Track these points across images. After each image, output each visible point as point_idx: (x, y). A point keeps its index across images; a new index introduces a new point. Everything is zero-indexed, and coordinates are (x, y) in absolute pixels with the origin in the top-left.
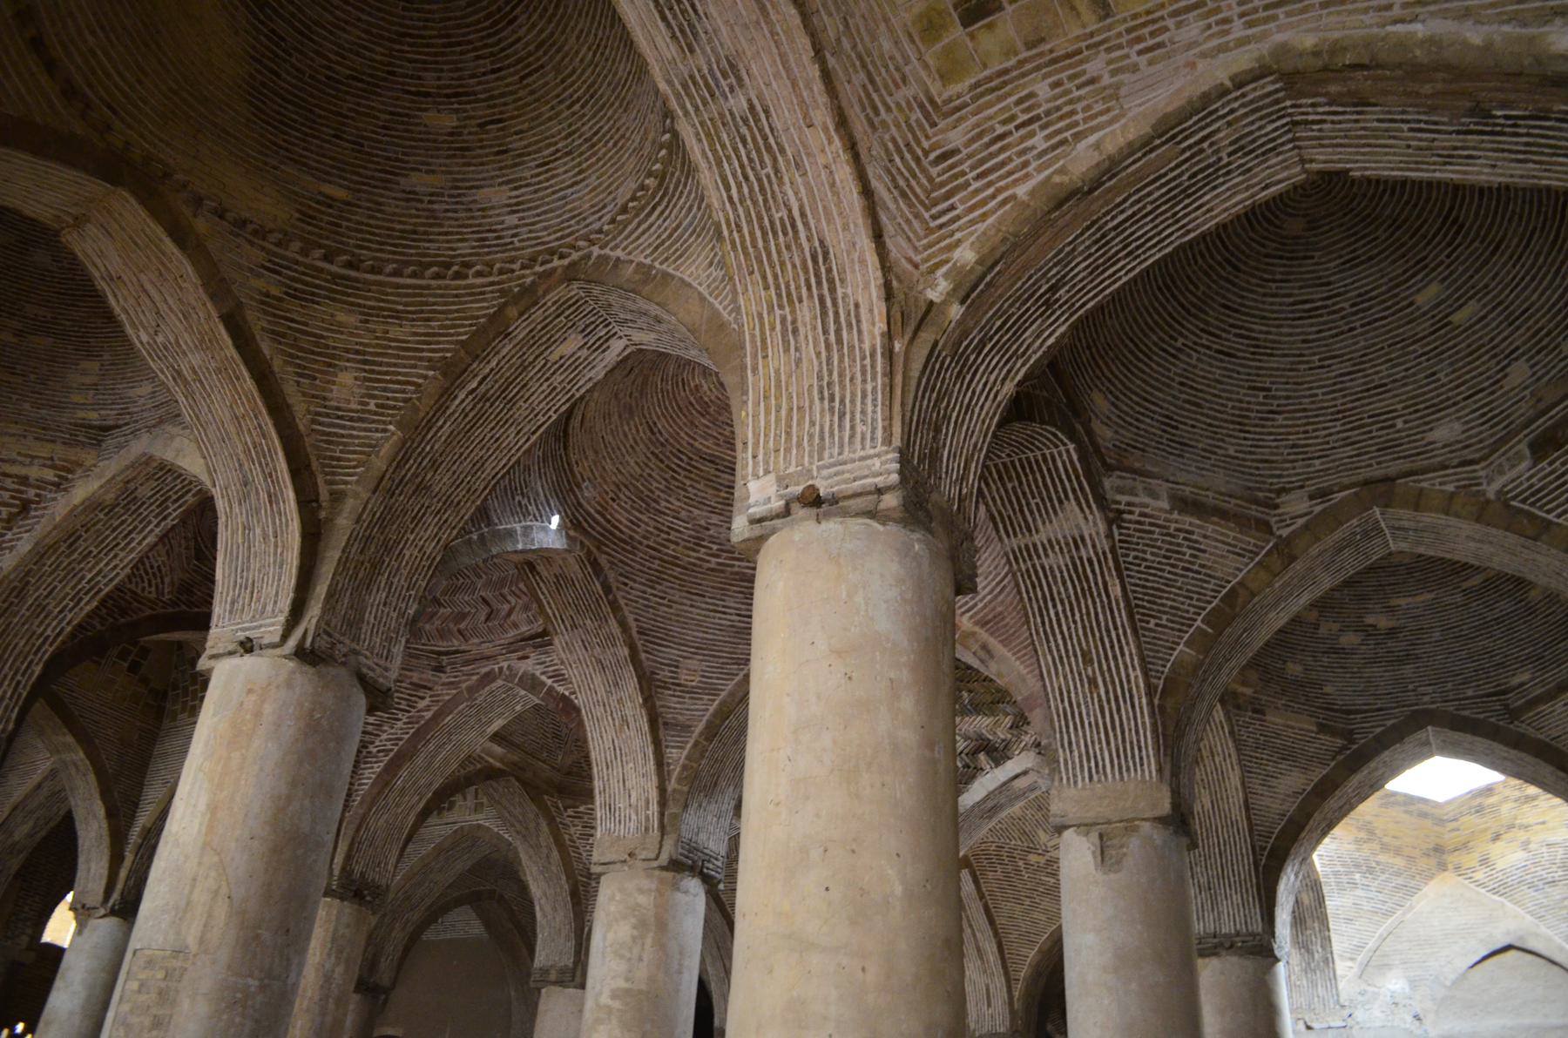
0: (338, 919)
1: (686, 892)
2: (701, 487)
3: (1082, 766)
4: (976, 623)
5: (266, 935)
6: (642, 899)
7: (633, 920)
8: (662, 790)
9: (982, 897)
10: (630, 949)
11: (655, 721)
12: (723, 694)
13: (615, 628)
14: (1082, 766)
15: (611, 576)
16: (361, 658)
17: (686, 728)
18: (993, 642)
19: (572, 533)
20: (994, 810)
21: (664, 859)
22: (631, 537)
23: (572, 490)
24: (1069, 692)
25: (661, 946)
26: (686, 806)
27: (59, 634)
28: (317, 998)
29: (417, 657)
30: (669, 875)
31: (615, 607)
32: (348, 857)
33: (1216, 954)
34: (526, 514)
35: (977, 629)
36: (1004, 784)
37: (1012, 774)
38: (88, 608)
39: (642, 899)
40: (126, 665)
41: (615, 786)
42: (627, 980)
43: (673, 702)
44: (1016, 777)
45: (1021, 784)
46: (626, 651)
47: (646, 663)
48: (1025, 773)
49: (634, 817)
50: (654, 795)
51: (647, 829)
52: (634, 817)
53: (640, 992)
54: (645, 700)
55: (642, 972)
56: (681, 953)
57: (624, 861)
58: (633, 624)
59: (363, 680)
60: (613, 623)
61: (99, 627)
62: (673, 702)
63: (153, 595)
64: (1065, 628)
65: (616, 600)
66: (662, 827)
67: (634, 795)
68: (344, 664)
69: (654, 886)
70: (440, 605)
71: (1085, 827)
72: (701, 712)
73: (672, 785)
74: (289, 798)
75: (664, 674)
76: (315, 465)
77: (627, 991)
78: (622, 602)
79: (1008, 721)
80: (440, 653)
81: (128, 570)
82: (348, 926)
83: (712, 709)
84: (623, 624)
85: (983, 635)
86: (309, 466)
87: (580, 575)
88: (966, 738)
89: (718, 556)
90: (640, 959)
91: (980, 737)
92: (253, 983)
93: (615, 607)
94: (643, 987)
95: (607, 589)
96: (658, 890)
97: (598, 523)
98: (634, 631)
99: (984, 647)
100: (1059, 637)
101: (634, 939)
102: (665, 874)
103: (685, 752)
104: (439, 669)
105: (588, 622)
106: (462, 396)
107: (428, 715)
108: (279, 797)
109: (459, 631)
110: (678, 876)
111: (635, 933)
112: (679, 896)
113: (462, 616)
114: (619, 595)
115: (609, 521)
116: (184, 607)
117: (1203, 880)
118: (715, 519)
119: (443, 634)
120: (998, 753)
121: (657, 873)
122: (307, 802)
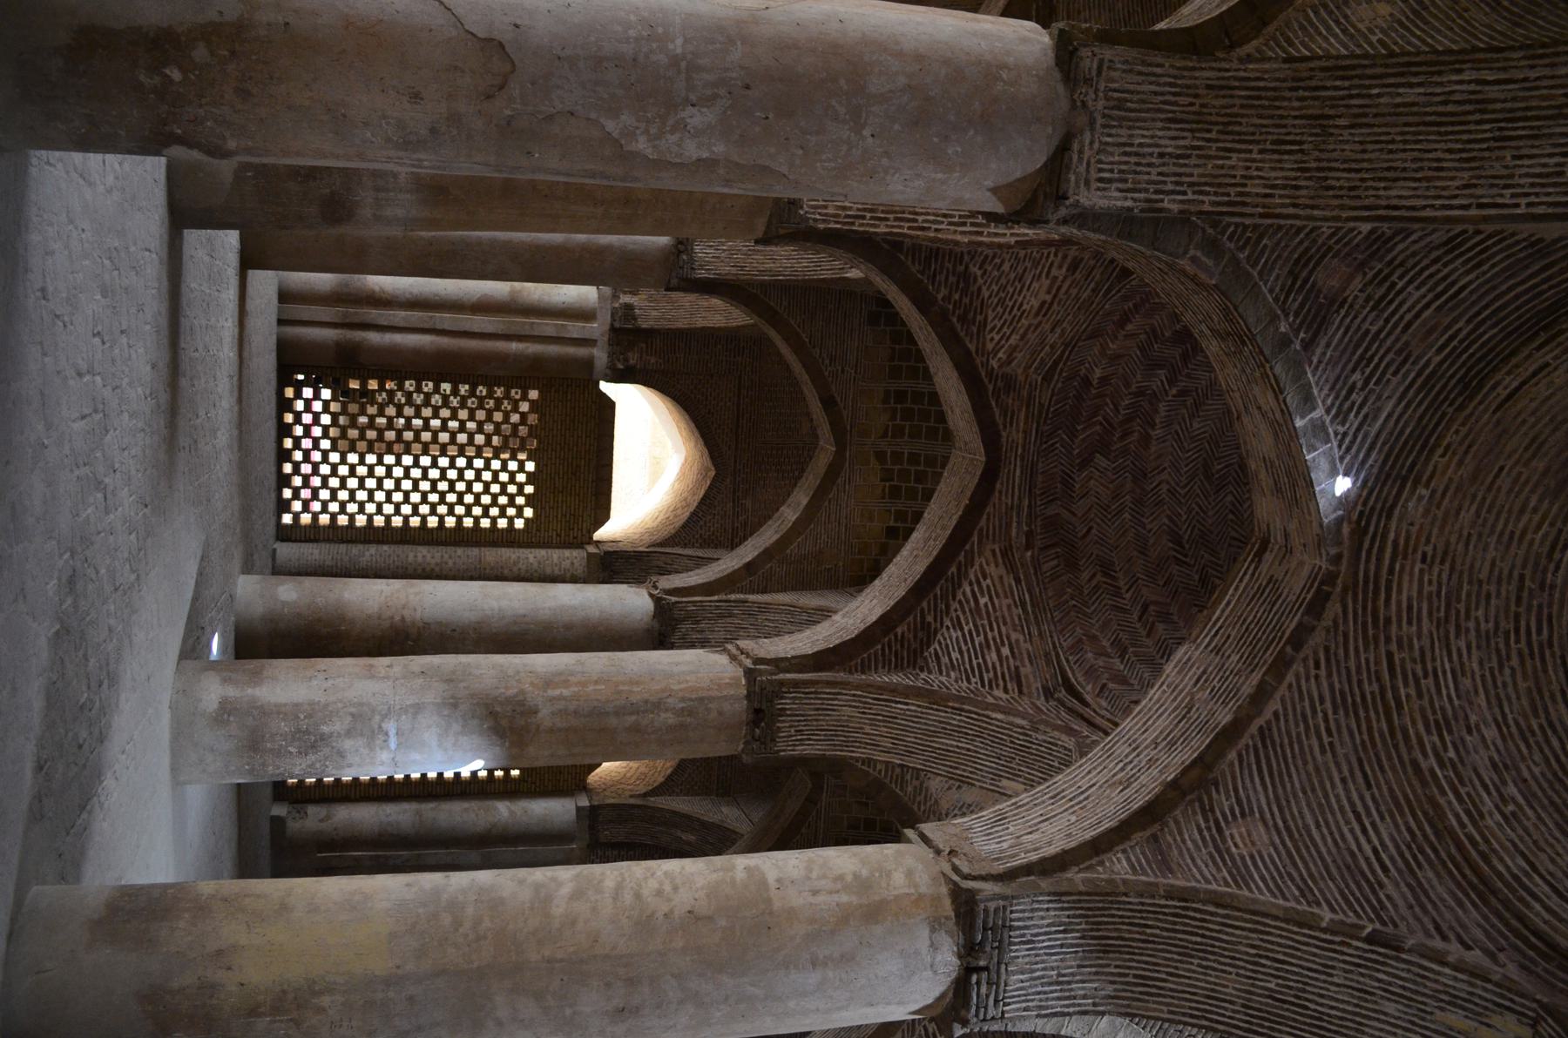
0: (725, 698)
1: (934, 946)
2: (1522, 685)
5: (736, 54)
7: (865, 873)
10: (824, 877)
11: (1150, 816)
13: (1248, 688)
15: (1317, 639)
16: (1087, 136)
17: (1165, 866)
19: (1346, 530)
22: (1388, 621)
23: (1405, 480)
25: (844, 918)
27: (923, 229)
28: (633, 699)
29: (1049, 662)
30: (947, 907)
31: (1280, 666)
32: (796, 684)
34: (1341, 416)
38: (959, 237)
39: (899, 878)
40: (892, 523)
41: (1034, 815)
42: (779, 880)
43: (1191, 835)
46: (1229, 718)
47: (1224, 767)
49: (1005, 845)
51: (997, 859)
52: (1005, 845)
53: (769, 901)
54: (1174, 785)
55: (797, 899)
57: (938, 852)
58: (1268, 714)
59: (1063, 149)
60: (1256, 677)
61: (940, 296)
62: (1191, 835)
63: (990, 346)
65: (1288, 664)
68: (1073, 106)
69: (923, 890)
70: (1122, 657)
72: (1197, 871)
74: (900, 54)
75: (1224, 802)
76: (1271, 29)
77: (763, 883)
78: (1290, 678)
80: (1066, 679)
81: (1013, 240)
82: (720, 713)
83: (1214, 887)
84: (1261, 695)
86: (1265, 24)
87: (1293, 598)
89: (1442, 765)
90: (815, 893)
92: (678, 46)
93: (1280, 666)
94: (777, 905)
95: (1297, 641)
96: (921, 897)
97: (1379, 560)
98: (1260, 721)
101: (841, 878)
104: (1048, 693)
105: (1235, 658)
106: (1465, 76)
107: (990, 700)
108: (897, 43)
109: (1104, 686)
110: (951, 924)
111: (849, 878)
113: (1124, 681)
114: (1297, 667)
115: (1391, 571)
116: (991, 387)
118: (1491, 733)
119: (1090, 673)
121: (944, 890)
122: (902, 80)
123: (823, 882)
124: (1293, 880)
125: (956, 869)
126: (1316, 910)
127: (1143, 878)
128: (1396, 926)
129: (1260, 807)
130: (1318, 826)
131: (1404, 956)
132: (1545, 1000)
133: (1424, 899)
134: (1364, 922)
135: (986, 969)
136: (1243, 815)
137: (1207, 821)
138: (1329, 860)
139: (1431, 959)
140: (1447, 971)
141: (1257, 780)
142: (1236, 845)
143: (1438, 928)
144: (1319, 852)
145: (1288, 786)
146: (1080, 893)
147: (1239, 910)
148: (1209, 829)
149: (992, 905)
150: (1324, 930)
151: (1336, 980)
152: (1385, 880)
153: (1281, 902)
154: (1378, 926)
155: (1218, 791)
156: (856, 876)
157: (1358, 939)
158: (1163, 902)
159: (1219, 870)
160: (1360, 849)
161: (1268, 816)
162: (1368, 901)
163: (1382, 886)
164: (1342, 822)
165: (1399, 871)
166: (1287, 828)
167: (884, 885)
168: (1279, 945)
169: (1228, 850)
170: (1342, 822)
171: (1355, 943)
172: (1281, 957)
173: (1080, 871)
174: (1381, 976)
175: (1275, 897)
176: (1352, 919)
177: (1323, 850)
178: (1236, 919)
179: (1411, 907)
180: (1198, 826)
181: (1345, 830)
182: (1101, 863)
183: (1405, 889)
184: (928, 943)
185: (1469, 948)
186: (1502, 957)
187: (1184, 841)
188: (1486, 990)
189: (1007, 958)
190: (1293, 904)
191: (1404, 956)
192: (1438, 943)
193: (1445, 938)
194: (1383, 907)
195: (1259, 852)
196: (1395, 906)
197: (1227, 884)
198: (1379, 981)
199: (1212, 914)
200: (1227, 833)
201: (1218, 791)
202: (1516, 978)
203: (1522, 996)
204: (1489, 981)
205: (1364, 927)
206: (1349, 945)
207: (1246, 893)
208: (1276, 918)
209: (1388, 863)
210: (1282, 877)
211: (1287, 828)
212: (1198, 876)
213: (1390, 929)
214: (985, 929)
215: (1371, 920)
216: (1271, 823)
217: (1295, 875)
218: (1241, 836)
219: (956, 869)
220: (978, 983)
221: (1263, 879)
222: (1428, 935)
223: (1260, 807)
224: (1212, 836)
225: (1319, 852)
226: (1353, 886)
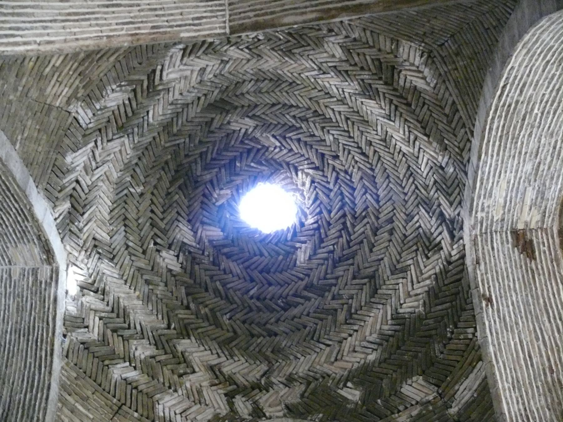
79: (103, 235)
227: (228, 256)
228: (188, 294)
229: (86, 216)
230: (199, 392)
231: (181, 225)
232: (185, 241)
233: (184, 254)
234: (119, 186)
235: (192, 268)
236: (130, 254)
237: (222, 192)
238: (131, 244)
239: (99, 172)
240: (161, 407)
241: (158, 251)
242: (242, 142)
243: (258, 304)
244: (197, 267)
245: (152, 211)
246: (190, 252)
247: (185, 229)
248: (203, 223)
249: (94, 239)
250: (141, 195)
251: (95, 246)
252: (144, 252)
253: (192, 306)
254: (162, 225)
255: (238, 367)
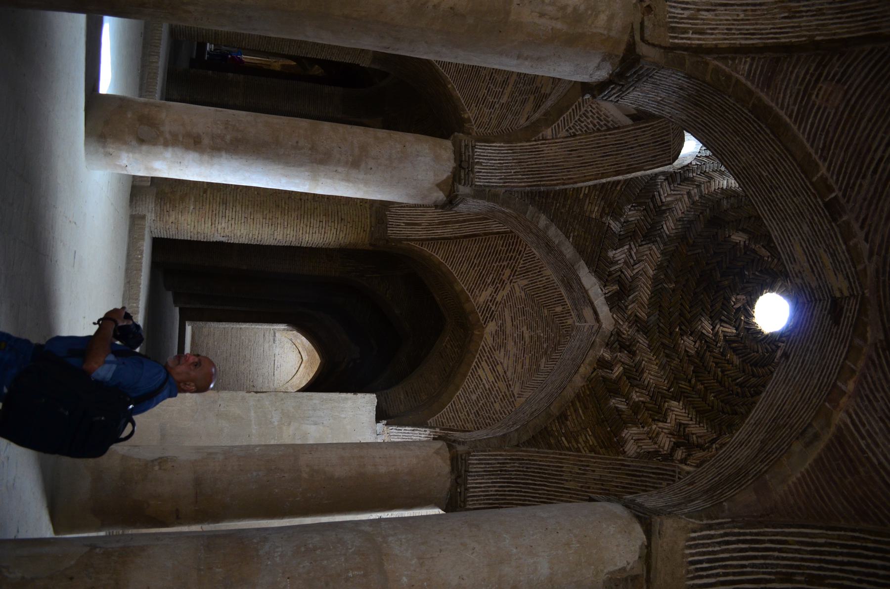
1: (598, 68)
3: (704, 553)
4: (839, 429)
6: (603, 18)
8: (714, 50)
9: (485, 234)
12: (795, 128)
14: (704, 553)
18: (821, 445)
20: (569, 286)
21: (643, 49)
24: (780, 550)
26: (689, 77)
30: (621, 51)
33: (452, 471)
35: (833, 429)
36: (592, 304)
37: (599, 310)
44: (596, 313)
45: (588, 313)
48: (597, 319)
49: (687, 13)
50: (709, 41)
51: (673, 30)
52: (687, 13)
56: (538, 59)
64: (855, 568)
66: (674, 48)
67: (709, 15)
69: (613, 33)
71: (647, 556)
73: (713, 62)
79: (643, 315)
83: (782, 113)
85: (827, 437)
88: (634, 278)
90: (542, 15)
91: (632, 290)
94: (513, 17)
99: (816, 437)
100: (846, 559)
101: (564, 8)
102: (623, 47)
103: (743, 80)
110: (617, 60)
111: (570, 10)
112: (597, 60)
117: (508, 467)
120: (615, 301)
121: (626, 38)
123: (550, 8)
124: (826, 137)
125: (642, 23)
126: (820, 163)
127: (749, 84)
128: (848, 202)
129: (852, 84)
130: (870, 120)
131: (833, 224)
132: (867, 295)
133: (875, 201)
134: (836, 187)
135: (623, 86)
136: (839, 81)
137: (815, 70)
138: (855, 142)
139: (843, 238)
140: (844, 247)
141: (866, 70)
142: (817, 96)
143: (865, 220)
144: (855, 133)
145: (879, 86)
146: (704, 82)
147: (780, 142)
148: (812, 75)
149: (647, 67)
150: (812, 183)
151: (795, 199)
152: (869, 176)
153: (808, 146)
154: (840, 194)
155: (838, 59)
156: (575, 9)
157: (822, 200)
158: (746, 111)
159: (795, 104)
160: (876, 151)
161: (851, 92)
162: (850, 178)
163: (864, 177)
164: (883, 130)
165: (880, 179)
166: (853, 107)
167: (589, 22)
168: (785, 168)
169: (811, 95)
170: (883, 130)
171: (819, 200)
172: (780, 171)
173: (715, 59)
174: (815, 218)
175: (808, 141)
176: (832, 181)
177: (858, 134)
178: (776, 144)
179: (865, 199)
180: (808, 70)
181: (880, 134)
182: (733, 59)
183: (872, 190)
184: (596, 65)
185: (866, 240)
186: (875, 258)
187: (792, 73)
188: (850, 268)
189: (637, 85)
190: (812, 151)
191: (833, 224)
192: (856, 227)
193: (862, 227)
194: (853, 188)
195: (825, 108)
196: (859, 192)
197: (790, 117)
198: (813, 218)
199: (766, 133)
200: (820, 85)
201: (838, 59)
202: (868, 273)
203: (861, 286)
204: (855, 268)
205: (830, 190)
206: (816, 198)
207: (795, 128)
208: (795, 160)
209: (880, 170)
210: (822, 131)
211: (853, 107)
212: (780, 101)
213: (843, 201)
214: (635, 73)
215: (840, 189)
216: (849, 96)
217: (831, 135)
218: (825, 92)
219: (642, 23)
220: (613, 89)
221: (812, 124)
222: (857, 219)
223: (852, 84)
224: (810, 81)
225: (855, 133)
226: (851, 165)
227: (735, 350)
228: (694, 372)
229: (631, 297)
230: (658, 434)
231: (703, 319)
232: (704, 331)
233: (701, 342)
234: (655, 280)
235: (704, 353)
236: (659, 332)
237: (739, 297)
238: (661, 325)
239: (638, 268)
240: (626, 431)
241: (682, 335)
242: (745, 253)
243: (739, 390)
244: (708, 354)
245: (681, 304)
246: (706, 341)
247: (706, 322)
248: (722, 321)
249: (636, 316)
250: (673, 290)
251: (636, 321)
252: (671, 334)
253: (693, 381)
254: (689, 316)
255: (697, 430)
